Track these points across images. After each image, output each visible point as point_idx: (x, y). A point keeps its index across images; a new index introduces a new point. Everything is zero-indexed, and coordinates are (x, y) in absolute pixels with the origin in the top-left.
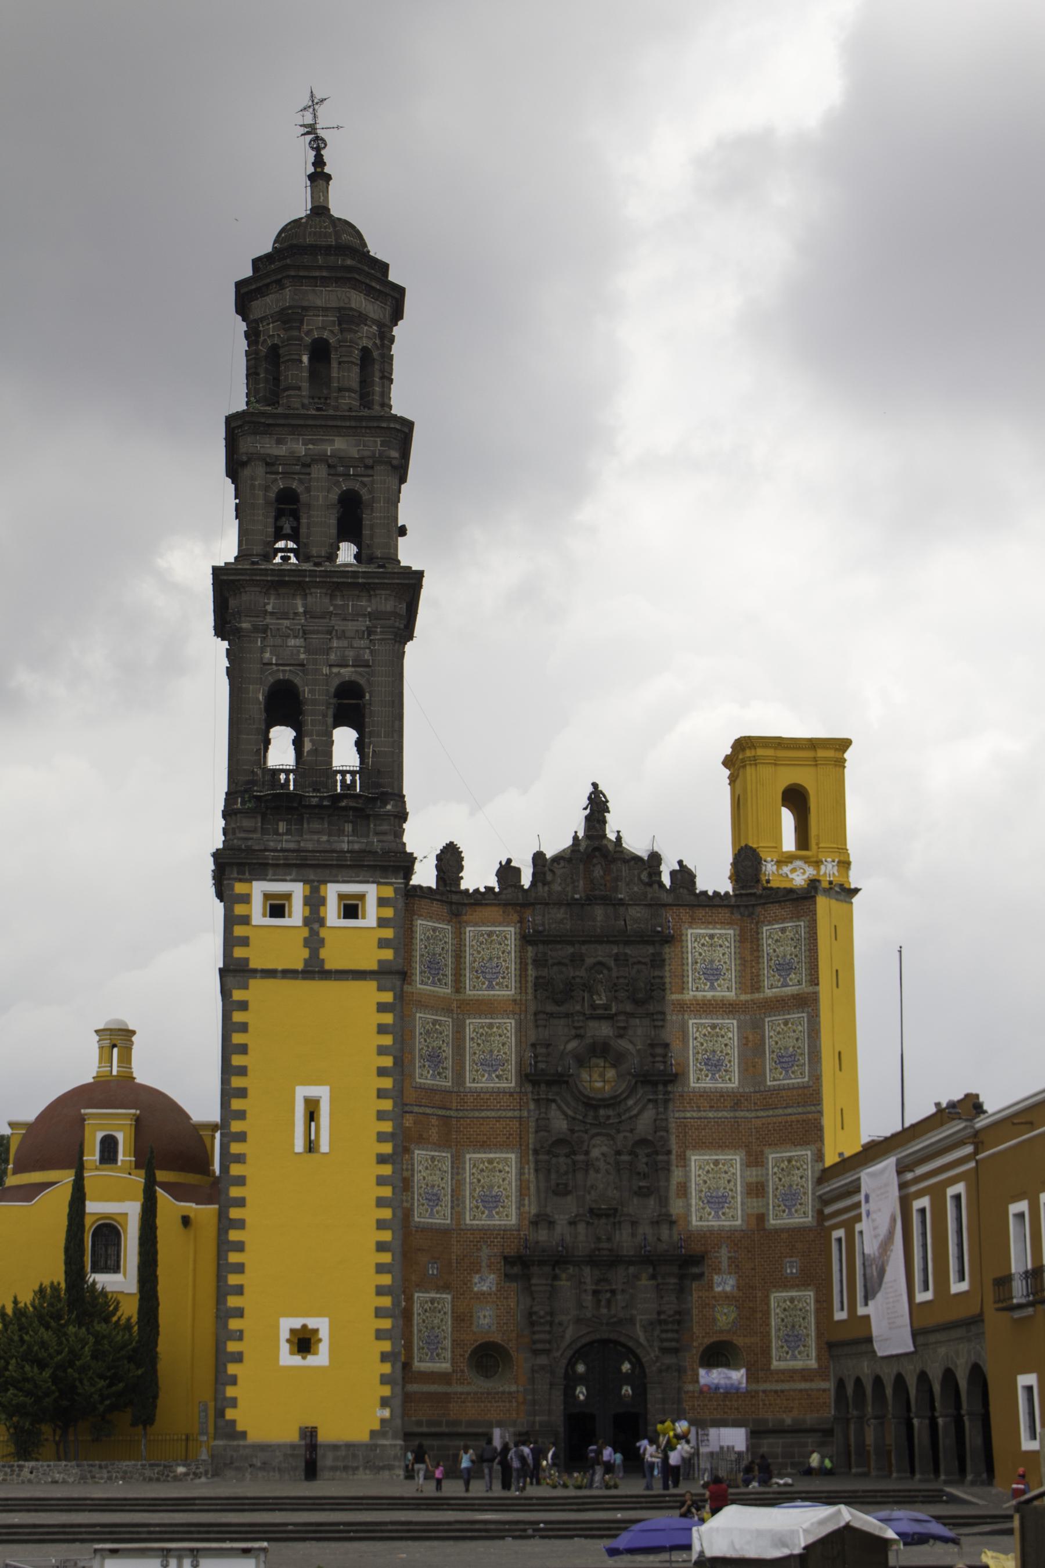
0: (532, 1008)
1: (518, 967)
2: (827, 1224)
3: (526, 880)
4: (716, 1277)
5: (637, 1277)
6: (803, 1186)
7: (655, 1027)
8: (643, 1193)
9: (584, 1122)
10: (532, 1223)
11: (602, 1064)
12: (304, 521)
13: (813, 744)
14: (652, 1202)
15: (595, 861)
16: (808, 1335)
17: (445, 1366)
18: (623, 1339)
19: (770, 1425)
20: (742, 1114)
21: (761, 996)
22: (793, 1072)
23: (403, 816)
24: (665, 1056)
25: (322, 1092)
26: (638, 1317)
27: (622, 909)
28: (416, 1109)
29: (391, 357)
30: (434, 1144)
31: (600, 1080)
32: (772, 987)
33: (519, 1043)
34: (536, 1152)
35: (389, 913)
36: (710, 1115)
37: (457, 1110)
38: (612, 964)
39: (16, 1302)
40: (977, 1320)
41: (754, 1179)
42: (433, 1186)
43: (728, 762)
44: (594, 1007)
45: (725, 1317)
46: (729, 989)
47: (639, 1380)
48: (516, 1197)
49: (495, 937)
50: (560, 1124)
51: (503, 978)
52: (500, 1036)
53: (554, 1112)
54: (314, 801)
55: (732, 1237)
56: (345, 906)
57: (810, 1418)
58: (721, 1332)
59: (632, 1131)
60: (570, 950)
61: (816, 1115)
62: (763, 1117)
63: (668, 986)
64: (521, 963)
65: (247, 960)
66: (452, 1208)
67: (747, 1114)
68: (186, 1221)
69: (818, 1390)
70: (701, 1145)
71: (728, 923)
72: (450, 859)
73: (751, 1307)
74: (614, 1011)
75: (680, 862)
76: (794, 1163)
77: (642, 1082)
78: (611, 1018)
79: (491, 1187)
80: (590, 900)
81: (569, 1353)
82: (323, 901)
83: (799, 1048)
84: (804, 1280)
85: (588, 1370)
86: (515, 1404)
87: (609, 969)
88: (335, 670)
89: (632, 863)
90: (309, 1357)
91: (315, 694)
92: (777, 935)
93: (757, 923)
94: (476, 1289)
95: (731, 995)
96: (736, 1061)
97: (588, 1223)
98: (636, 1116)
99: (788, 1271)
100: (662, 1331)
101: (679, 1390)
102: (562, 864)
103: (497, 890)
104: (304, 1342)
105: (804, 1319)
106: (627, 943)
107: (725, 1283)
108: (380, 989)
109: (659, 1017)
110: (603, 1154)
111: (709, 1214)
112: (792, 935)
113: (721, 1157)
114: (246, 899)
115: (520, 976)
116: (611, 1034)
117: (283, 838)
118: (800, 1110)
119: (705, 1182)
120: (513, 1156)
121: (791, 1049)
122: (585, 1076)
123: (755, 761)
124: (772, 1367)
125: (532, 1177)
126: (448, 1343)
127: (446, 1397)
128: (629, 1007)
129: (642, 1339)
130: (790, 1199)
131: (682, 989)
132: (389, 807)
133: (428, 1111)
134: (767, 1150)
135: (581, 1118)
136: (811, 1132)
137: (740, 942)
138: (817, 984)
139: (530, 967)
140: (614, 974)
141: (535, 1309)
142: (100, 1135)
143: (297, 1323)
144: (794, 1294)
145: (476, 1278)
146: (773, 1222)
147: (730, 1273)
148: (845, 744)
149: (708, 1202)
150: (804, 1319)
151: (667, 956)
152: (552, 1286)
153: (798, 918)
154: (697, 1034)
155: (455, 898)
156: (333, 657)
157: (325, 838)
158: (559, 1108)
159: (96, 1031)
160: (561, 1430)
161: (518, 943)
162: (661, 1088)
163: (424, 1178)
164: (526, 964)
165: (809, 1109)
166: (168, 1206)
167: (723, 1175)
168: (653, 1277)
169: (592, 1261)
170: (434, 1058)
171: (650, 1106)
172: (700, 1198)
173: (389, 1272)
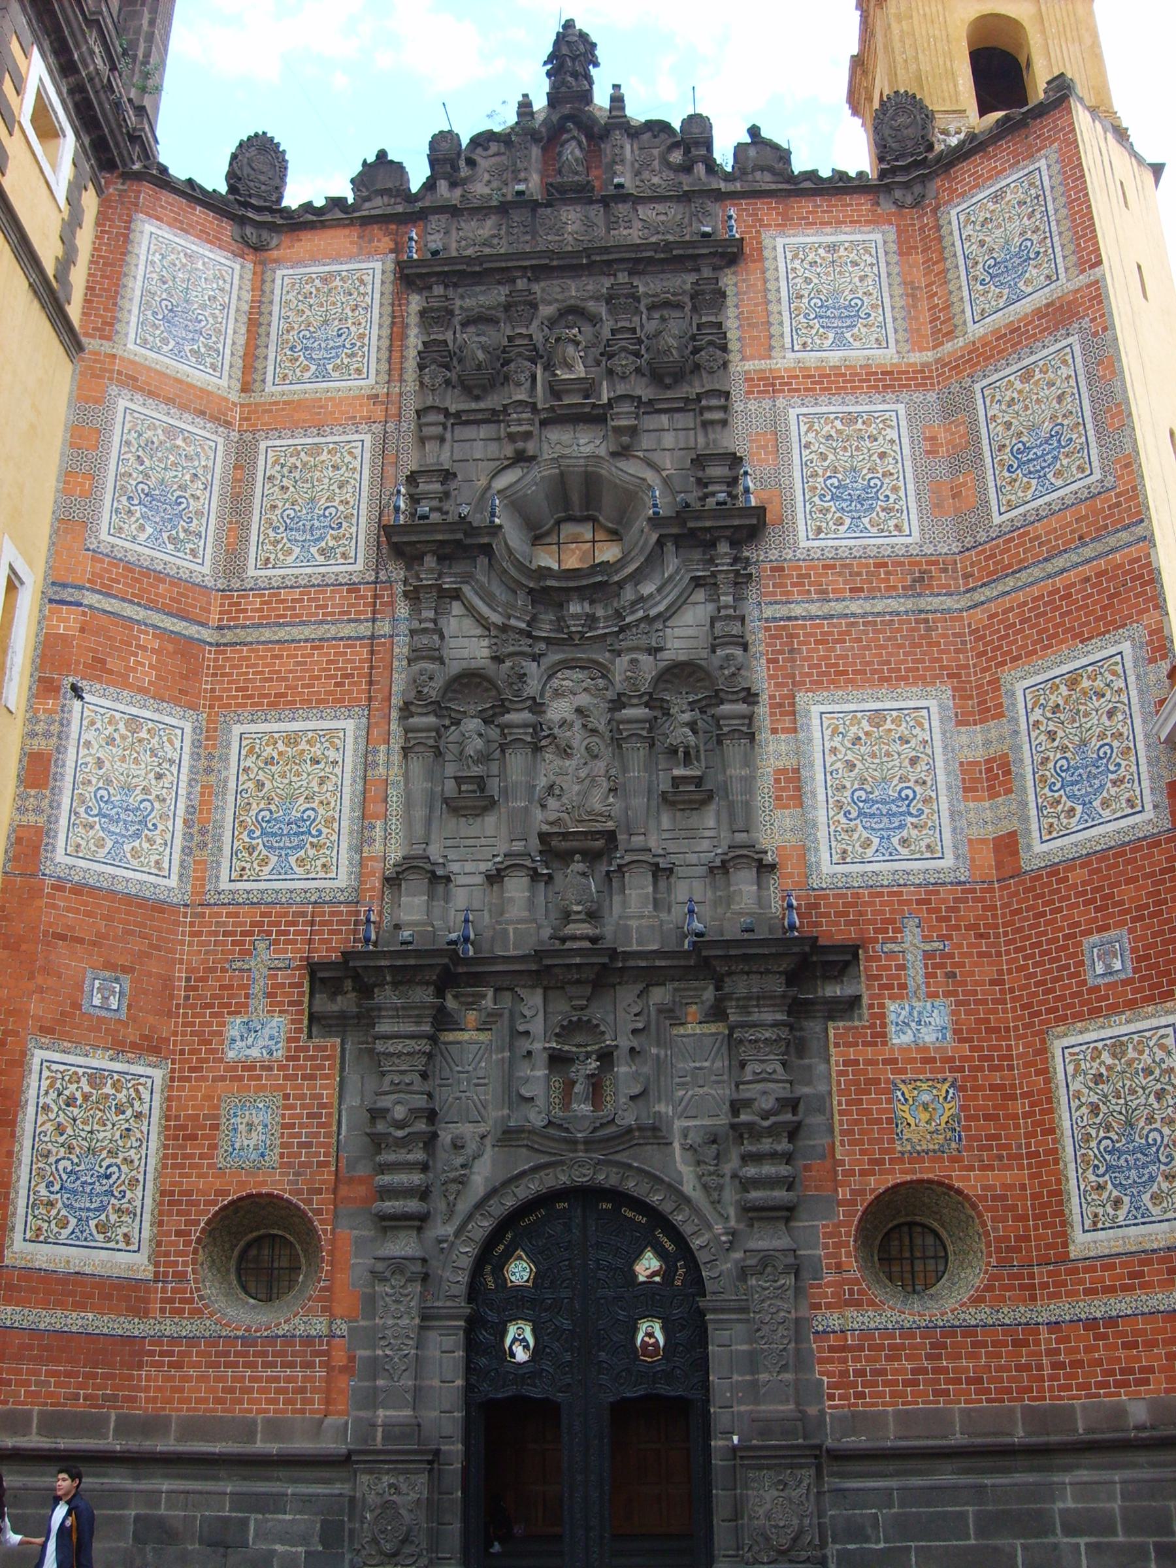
0: (411, 405)
1: (386, 332)
4: (892, 1006)
5: (671, 1015)
7: (705, 424)
8: (689, 797)
9: (529, 635)
11: (589, 536)
14: (711, 823)
15: (565, 136)
17: (133, 1263)
20: (936, 602)
21: (960, 342)
22: (1059, 474)
24: (734, 481)
26: (678, 1124)
27: (622, 209)
28: (91, 599)
30: (142, 690)
36: (855, 607)
37: (220, 628)
38: (603, 310)
41: (979, 755)
42: (128, 789)
48: (352, 819)
49: (338, 282)
50: (468, 647)
51: (353, 355)
52: (336, 467)
53: (456, 622)
55: (934, 904)
58: (917, 1156)
59: (654, 651)
62: (990, 600)
63: (733, 346)
64: (393, 324)
66: (187, 851)
67: (949, 602)
70: (836, 677)
71: (868, 222)
72: (259, 160)
73: (1001, 1087)
75: (754, 131)
77: (678, 540)
78: (596, 417)
79: (293, 798)
81: (482, 1227)
86: (320, 1373)
87: (594, 320)
89: (647, 136)
92: (984, 214)
93: (938, 207)
94: (231, 1054)
95: (888, 356)
96: (911, 487)
97: (535, 876)
100: (746, 1158)
101: (800, 1327)
102: (494, 147)
103: (350, 201)
107: (918, 1022)
109: (714, 402)
110: (579, 711)
111: (867, 844)
113: (888, 705)
115: (390, 349)
116: (602, 452)
118: (1087, 552)
119: (851, 766)
120: (349, 725)
121: (1047, 425)
124: (1074, 1252)
126: (145, 1198)
127: (131, 1350)
128: (643, 390)
129: (689, 1186)
130: (1083, 776)
133: (129, 611)
134: (1007, 675)
135: (523, 625)
137: (900, 254)
138: (1099, 263)
141: (385, 1102)
144: (1120, 1027)
145: (234, 1027)
146: (1040, 850)
147: (933, 995)
151: (730, 291)
152: (433, 1039)
154: (811, 437)
158: (471, 610)
161: (389, 288)
162: (723, 548)
163: (100, 763)
164: (405, 326)
165: (1112, 541)
167: (897, 747)
168: (717, 1013)
169: (545, 970)
171: (700, 595)
172: (839, 805)
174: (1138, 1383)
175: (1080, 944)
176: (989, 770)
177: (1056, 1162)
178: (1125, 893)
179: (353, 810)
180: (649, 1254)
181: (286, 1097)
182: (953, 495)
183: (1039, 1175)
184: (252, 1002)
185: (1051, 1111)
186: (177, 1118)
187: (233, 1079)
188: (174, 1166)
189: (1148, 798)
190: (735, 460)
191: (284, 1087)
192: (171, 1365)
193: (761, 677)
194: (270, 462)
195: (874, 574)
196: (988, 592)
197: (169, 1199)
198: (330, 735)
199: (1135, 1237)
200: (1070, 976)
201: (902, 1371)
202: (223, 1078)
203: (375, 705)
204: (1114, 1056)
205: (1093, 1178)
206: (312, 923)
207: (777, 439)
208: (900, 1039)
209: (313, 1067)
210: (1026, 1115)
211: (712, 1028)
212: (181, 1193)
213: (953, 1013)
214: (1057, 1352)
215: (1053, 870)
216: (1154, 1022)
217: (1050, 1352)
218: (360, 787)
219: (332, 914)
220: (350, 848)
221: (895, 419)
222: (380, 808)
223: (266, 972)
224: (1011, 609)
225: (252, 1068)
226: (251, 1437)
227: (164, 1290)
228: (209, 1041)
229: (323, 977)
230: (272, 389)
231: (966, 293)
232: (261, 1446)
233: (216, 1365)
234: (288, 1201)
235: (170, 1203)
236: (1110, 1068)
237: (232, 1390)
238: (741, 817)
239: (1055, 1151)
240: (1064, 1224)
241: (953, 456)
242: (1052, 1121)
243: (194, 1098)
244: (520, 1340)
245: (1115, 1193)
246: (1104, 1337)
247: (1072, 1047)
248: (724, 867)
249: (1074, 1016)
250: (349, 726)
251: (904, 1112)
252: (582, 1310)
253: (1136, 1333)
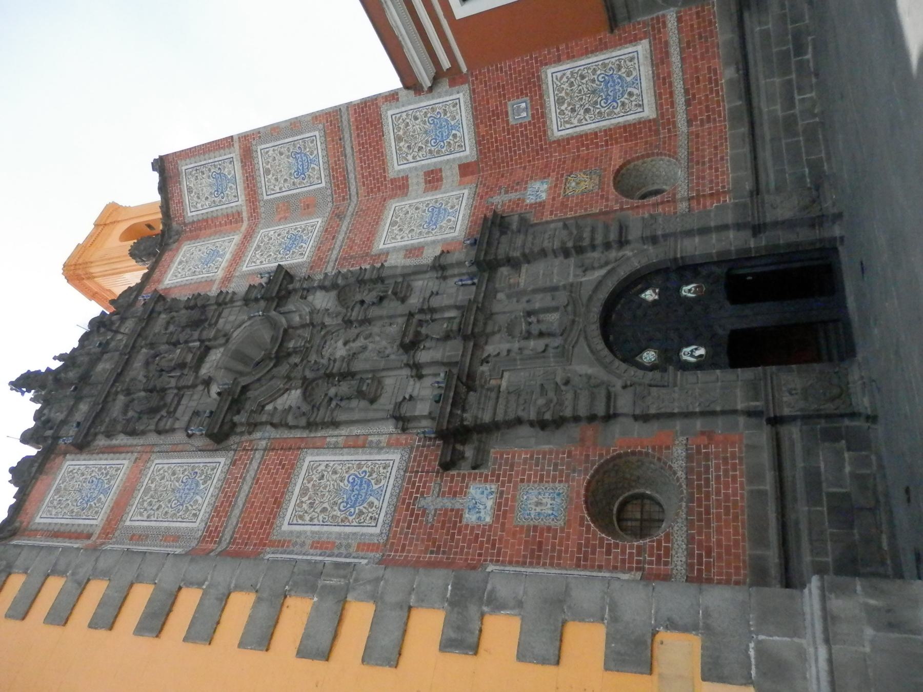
6: (426, 113)
10: (404, 430)
16: (604, 65)
18: (603, 295)
19: (739, 103)
21: (244, 208)
26: (571, 279)
36: (341, 238)
45: (581, 183)
52: (163, 478)
61: (351, 112)
69: (680, 30)
76: (401, 133)
77: (278, 306)
78: (206, 350)
79: (338, 490)
83: (288, 150)
84: (532, 87)
93: (185, 224)
94: (488, 519)
95: (237, 238)
99: (524, 114)
105: (583, 77)
107: (538, 191)
110: (345, 344)
112: (193, 179)
118: (347, 136)
125: (344, 431)
134: (391, 175)
138: (232, 137)
144: (551, 101)
145: (470, 518)
146: (468, 152)
149: (435, 224)
150: (583, 77)
153: (178, 174)
158: (273, 399)
165: (345, 123)
174: (716, 74)
175: (512, 126)
176: (430, 182)
177: (610, 130)
178: (493, 104)
179: (357, 453)
180: (643, 296)
181: (522, 481)
182: (308, 206)
183: (616, 139)
184: (457, 506)
185: (586, 135)
186: (525, 556)
187: (505, 517)
188: (559, 558)
189: (454, 97)
190: (251, 287)
191: (515, 487)
192: (709, 555)
194: (140, 518)
195: (329, 233)
196: (353, 188)
199: (646, 84)
200: (526, 130)
201: (710, 175)
202: (503, 524)
203: (303, 445)
204: (563, 103)
205: (618, 109)
206: (417, 472)
209: (506, 465)
210: (588, 149)
211: (525, 267)
212: (579, 551)
213: (535, 180)
214: (702, 120)
215: (478, 143)
216: (550, 83)
217: (702, 124)
218: (346, 450)
219: (414, 461)
220: (379, 453)
222: (362, 438)
223: (440, 499)
224: (363, 174)
225: (500, 505)
226: (762, 493)
227: (651, 563)
228: (477, 535)
231: (224, 206)
232: (768, 485)
233: (708, 522)
234: (593, 476)
235: (586, 560)
236: (569, 104)
237: (727, 509)
239: (605, 131)
240: (640, 123)
242: (591, 134)
243: (513, 545)
244: (692, 353)
245: (626, 96)
246: (694, 95)
247: (559, 127)
249: (544, 126)
251: (579, 190)
253: (692, 78)
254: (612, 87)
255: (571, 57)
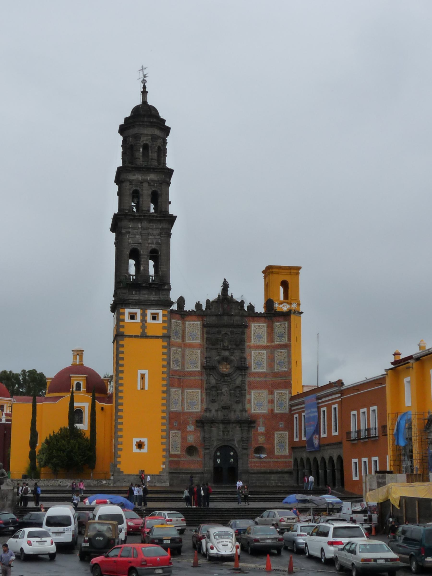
2: (292, 412)
3: (204, 308)
5: (235, 427)
8: (238, 402)
12: (141, 199)
13: (290, 268)
17: (179, 453)
18: (230, 445)
23: (169, 289)
24: (245, 361)
25: (146, 372)
29: (166, 149)
31: (225, 369)
32: (277, 341)
33: (202, 357)
34: (206, 390)
35: (166, 319)
36: (258, 379)
38: (229, 333)
39: (54, 433)
40: (340, 443)
43: (264, 272)
44: (224, 346)
46: (264, 342)
47: (236, 457)
50: (213, 381)
54: (144, 285)
55: (264, 416)
56: (153, 316)
57: (286, 469)
60: (217, 329)
65: (124, 332)
68: (102, 409)
69: (289, 461)
74: (230, 348)
75: (250, 303)
78: (228, 350)
79: (193, 400)
80: (224, 314)
81: (216, 449)
82: (146, 315)
84: (285, 429)
85: (220, 455)
88: (150, 245)
90: (142, 450)
91: (144, 252)
92: (279, 326)
93: (273, 322)
98: (236, 379)
104: (140, 445)
106: (234, 327)
107: (261, 429)
108: (163, 341)
114: (123, 314)
116: (229, 354)
117: (134, 296)
118: (285, 378)
120: (199, 391)
122: (221, 367)
123: (273, 273)
126: (180, 446)
128: (234, 347)
129: (237, 445)
130: (281, 405)
131: (250, 341)
132: (166, 287)
133: (174, 377)
136: (287, 385)
139: (205, 334)
140: (230, 337)
142: (75, 382)
143: (138, 440)
145: (188, 427)
146: (276, 411)
148: (299, 268)
155: (183, 313)
156: (149, 241)
157: (147, 296)
158: (213, 376)
159: (72, 351)
160: (213, 472)
162: (243, 371)
166: (99, 404)
168: (240, 427)
170: (176, 361)
173: (165, 425)
182: (271, 365)
193: (247, 387)
195: (261, 375)
197: (182, 446)
198: (197, 392)
207: (250, 356)
208: (259, 431)
211: (240, 429)
221: (265, 353)
229: (197, 422)
230: (187, 341)
238: (244, 405)
241: (271, 359)
244: (218, 461)
247: (277, 434)
248: (242, 411)
250: (199, 391)
252: (225, 458)
254: (282, 446)
255: (289, 438)
